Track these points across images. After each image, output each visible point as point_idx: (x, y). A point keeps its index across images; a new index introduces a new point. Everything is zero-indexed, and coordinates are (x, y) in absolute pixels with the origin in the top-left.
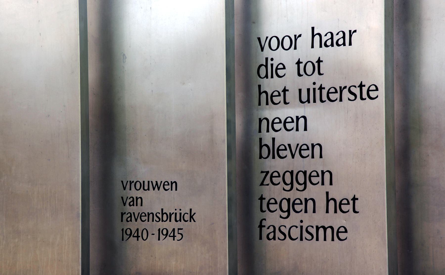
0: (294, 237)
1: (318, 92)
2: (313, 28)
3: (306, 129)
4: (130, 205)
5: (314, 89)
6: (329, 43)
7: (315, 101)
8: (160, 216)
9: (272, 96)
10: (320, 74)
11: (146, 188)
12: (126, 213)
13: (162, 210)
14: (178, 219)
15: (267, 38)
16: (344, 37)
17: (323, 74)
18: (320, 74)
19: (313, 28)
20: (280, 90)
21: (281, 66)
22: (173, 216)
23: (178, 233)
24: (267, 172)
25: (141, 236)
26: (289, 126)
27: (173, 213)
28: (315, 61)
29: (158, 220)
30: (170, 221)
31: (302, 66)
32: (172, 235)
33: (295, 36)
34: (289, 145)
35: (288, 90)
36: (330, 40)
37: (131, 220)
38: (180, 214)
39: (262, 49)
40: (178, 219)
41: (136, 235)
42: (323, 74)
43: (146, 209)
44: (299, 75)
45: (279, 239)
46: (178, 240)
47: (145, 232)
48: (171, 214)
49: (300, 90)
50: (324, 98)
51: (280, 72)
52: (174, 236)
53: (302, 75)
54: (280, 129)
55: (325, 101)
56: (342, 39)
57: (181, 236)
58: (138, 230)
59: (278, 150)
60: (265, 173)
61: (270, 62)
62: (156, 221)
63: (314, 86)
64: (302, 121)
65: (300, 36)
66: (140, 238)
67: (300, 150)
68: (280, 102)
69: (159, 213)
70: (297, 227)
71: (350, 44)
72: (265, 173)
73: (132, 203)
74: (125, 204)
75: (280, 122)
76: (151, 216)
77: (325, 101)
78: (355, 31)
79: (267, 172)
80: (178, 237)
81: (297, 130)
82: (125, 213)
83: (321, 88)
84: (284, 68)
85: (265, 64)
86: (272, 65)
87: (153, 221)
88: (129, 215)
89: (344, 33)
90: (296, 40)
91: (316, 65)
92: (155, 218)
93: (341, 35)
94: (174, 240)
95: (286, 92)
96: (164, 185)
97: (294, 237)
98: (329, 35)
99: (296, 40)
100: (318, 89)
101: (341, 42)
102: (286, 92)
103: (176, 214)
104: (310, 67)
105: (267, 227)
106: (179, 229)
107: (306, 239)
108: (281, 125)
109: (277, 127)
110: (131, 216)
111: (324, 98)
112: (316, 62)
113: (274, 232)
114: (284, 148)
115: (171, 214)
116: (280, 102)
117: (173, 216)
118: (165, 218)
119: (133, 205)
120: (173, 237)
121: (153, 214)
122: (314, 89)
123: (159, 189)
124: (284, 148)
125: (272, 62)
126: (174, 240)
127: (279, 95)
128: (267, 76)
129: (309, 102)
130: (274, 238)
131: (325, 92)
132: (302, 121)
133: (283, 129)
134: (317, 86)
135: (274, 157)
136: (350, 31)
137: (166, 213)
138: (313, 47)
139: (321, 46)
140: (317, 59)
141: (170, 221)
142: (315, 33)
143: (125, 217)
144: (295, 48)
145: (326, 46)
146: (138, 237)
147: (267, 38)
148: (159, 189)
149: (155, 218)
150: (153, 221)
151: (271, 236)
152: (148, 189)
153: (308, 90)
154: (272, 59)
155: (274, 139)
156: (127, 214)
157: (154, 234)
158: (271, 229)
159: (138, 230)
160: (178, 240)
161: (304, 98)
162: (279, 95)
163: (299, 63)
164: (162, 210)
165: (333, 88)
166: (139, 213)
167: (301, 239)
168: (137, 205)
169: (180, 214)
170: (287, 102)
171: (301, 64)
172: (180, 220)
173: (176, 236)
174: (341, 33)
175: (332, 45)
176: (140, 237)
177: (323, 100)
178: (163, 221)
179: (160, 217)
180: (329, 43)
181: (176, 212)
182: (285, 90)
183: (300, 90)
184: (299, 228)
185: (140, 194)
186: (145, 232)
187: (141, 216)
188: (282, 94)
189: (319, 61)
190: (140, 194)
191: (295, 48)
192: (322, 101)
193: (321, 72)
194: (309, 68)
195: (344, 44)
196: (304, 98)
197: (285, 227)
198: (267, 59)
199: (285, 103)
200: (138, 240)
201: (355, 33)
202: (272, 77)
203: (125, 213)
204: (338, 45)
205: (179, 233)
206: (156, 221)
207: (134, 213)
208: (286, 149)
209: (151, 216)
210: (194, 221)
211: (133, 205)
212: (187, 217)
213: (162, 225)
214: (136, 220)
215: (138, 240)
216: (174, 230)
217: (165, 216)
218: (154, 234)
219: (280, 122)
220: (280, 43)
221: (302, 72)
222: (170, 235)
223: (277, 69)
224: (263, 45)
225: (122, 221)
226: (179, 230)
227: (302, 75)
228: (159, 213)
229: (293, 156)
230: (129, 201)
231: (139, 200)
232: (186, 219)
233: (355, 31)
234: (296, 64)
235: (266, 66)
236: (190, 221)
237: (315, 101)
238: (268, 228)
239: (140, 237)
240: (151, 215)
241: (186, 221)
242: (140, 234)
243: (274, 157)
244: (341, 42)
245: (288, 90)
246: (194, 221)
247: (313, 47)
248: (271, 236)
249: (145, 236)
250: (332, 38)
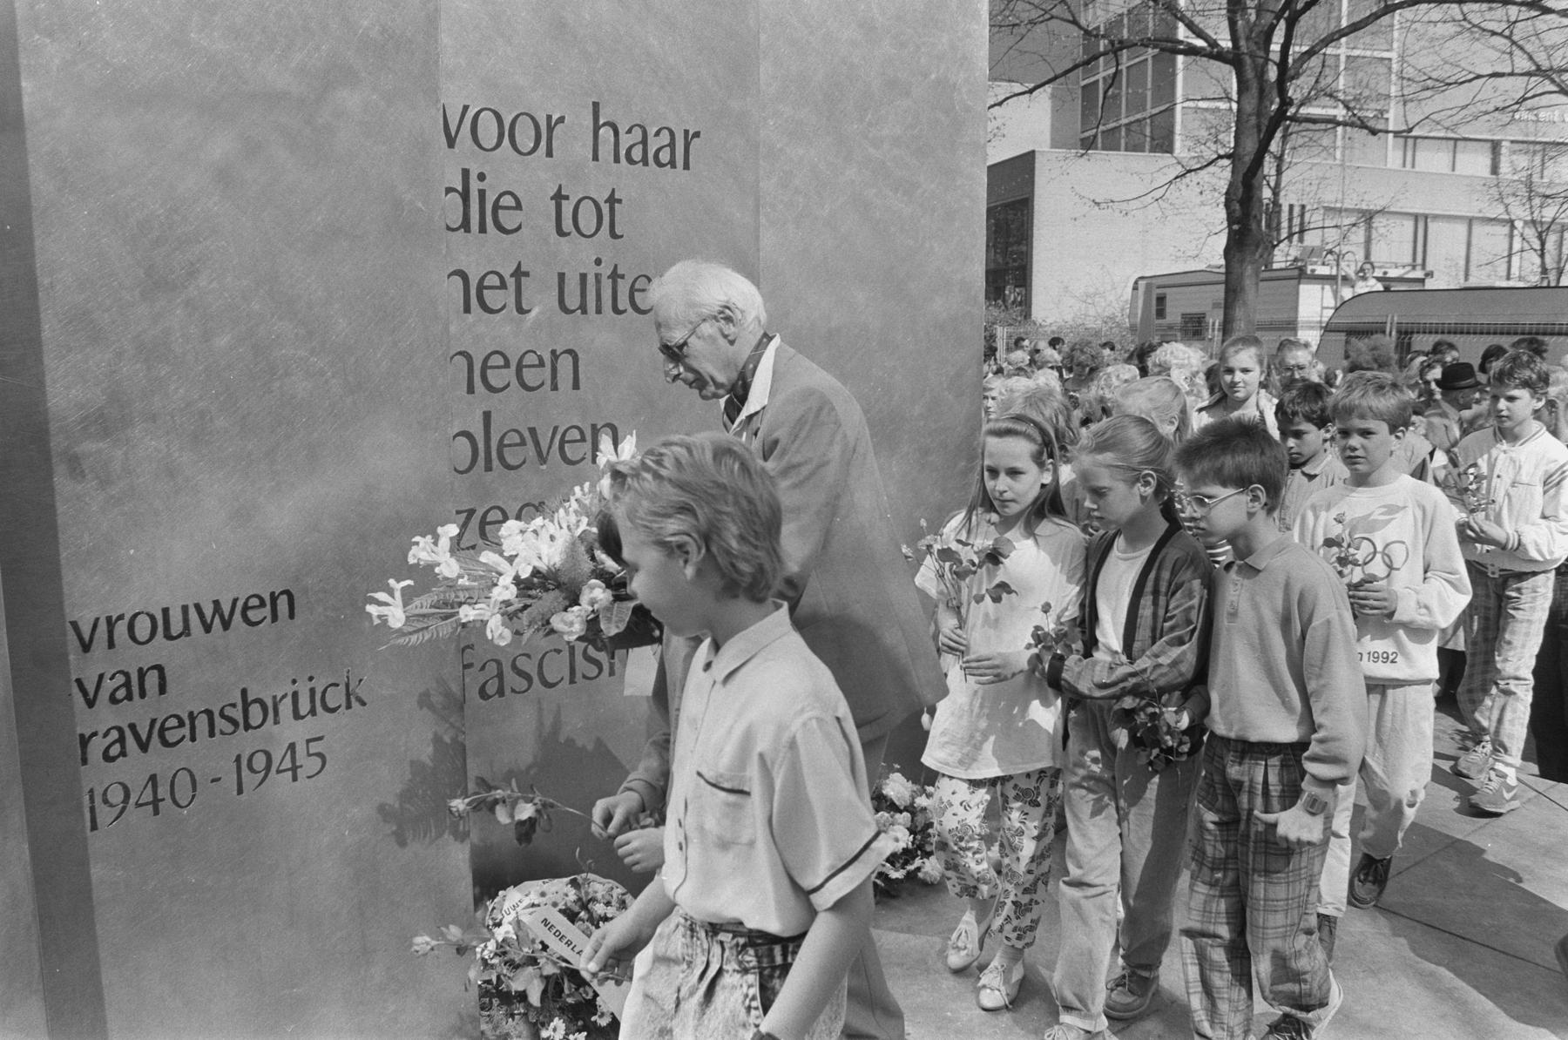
0: (550, 679)
1: (607, 285)
2: (596, 105)
3: (576, 386)
4: (114, 700)
5: (598, 277)
6: (637, 154)
7: (599, 311)
8: (237, 714)
9: (481, 287)
10: (614, 235)
11: (176, 626)
12: (101, 734)
13: (244, 692)
14: (304, 707)
15: (466, 108)
16: (672, 145)
17: (622, 236)
18: (614, 235)
19: (596, 105)
20: (507, 272)
21: (507, 201)
22: (286, 707)
23: (309, 755)
24: (471, 512)
25: (169, 801)
26: (530, 376)
27: (284, 696)
28: (602, 197)
29: (229, 728)
30: (276, 722)
31: (568, 208)
32: (287, 764)
33: (549, 117)
34: (532, 431)
35: (527, 274)
36: (641, 146)
37: (123, 753)
38: (312, 691)
39: (451, 142)
40: (304, 707)
41: (148, 796)
42: (622, 236)
43: (182, 699)
44: (561, 232)
45: (513, 691)
46: (309, 777)
47: (183, 780)
48: (278, 698)
49: (562, 276)
50: (623, 303)
51: (507, 218)
52: (294, 769)
53: (569, 234)
54: (508, 385)
55: (625, 311)
56: (668, 149)
57: (318, 761)
58: (153, 778)
59: (501, 445)
60: (465, 514)
61: (475, 185)
62: (222, 733)
63: (599, 269)
64: (565, 363)
65: (561, 120)
66: (164, 806)
67: (563, 442)
68: (504, 307)
69: (234, 705)
70: (558, 651)
71: (686, 166)
72: (465, 514)
73: (121, 694)
74: (91, 703)
75: (507, 365)
76: (202, 723)
77: (625, 311)
78: (697, 135)
79: (471, 512)
80: (310, 765)
81: (555, 387)
82: (95, 734)
83: (615, 276)
84: (518, 206)
85: (460, 189)
86: (482, 193)
87: (212, 734)
88: (115, 735)
89: (672, 134)
90: (550, 129)
91: (605, 209)
92: (220, 724)
93: (665, 138)
94: (295, 779)
95: (523, 279)
96: (246, 608)
97: (551, 680)
98: (638, 133)
99: (550, 129)
100: (609, 277)
101: (665, 156)
102: (523, 279)
103: (295, 695)
104: (587, 211)
105: (478, 666)
106: (308, 741)
107: (584, 677)
108: (509, 376)
109: (495, 378)
110: (121, 740)
111: (623, 303)
112: (606, 202)
113: (500, 676)
114: (518, 440)
115: (278, 698)
116: (504, 307)
117: (286, 707)
118: (256, 718)
119: (129, 697)
120: (290, 773)
121: (209, 713)
122: (598, 276)
123: (226, 625)
124: (518, 440)
125: (482, 185)
126: (295, 779)
127: (503, 286)
128: (466, 225)
129: (584, 312)
130: (501, 692)
131: (624, 288)
132: (565, 363)
133: (514, 382)
134: (606, 270)
135: (489, 468)
136: (686, 132)
137: (259, 701)
138: (596, 158)
139: (617, 160)
140: (606, 196)
141: (276, 722)
142: (601, 122)
143: (96, 747)
144: (549, 154)
145: (630, 161)
146: (156, 802)
147: (466, 108)
148: (226, 625)
149: (218, 720)
150: (212, 734)
151: (492, 688)
152: (186, 631)
153: (583, 277)
154: (482, 177)
155: (487, 416)
156: (106, 735)
157: (213, 781)
158: (492, 669)
159: (153, 778)
160: (309, 777)
161: (573, 301)
162: (503, 286)
163: (559, 197)
164: (244, 692)
165: (643, 278)
166: (153, 722)
167: (572, 681)
168: (143, 694)
169: (312, 691)
170: (525, 307)
171: (564, 203)
172: (313, 712)
173: (301, 766)
174: (665, 134)
175: (645, 161)
176: (163, 800)
177: (621, 307)
178: (247, 727)
179: (237, 714)
180: (637, 154)
181: (290, 689)
182: (519, 273)
183: (562, 276)
184: (566, 654)
185: (160, 653)
186: (183, 778)
187: (163, 729)
188: (511, 282)
189: (612, 200)
190: (160, 653)
191: (549, 154)
192: (616, 311)
193: (618, 231)
194: (587, 220)
195: (672, 163)
196: (573, 301)
197: (528, 656)
198: (466, 173)
199: (521, 310)
200: (156, 812)
201: (695, 139)
202: (483, 229)
203: (95, 734)
204: (659, 164)
205: (311, 752)
206: (222, 733)
207: (132, 727)
208: (523, 443)
209: (202, 723)
210: (363, 704)
211: (129, 697)
212: (335, 697)
213: (245, 742)
214: (144, 746)
215: (156, 812)
216: (292, 747)
217: (255, 710)
218: (213, 781)
219: (507, 365)
220: (508, 133)
221: (567, 224)
222: (281, 768)
223: (496, 207)
224: (453, 134)
225: (84, 761)
226: (311, 744)
227: (569, 234)
228: (234, 705)
229: (542, 459)
230: (108, 685)
231: (152, 680)
232: (331, 705)
233: (697, 135)
234: (552, 198)
235: (465, 196)
236: (349, 706)
237: (599, 311)
238: (483, 668)
239: (163, 800)
240: (204, 719)
241: (333, 710)
242: (163, 791)
243: (489, 468)
244: (665, 156)
245: (527, 274)
246: (363, 704)
247: (596, 158)
248: (492, 688)
249: (183, 795)
250: (644, 142)
